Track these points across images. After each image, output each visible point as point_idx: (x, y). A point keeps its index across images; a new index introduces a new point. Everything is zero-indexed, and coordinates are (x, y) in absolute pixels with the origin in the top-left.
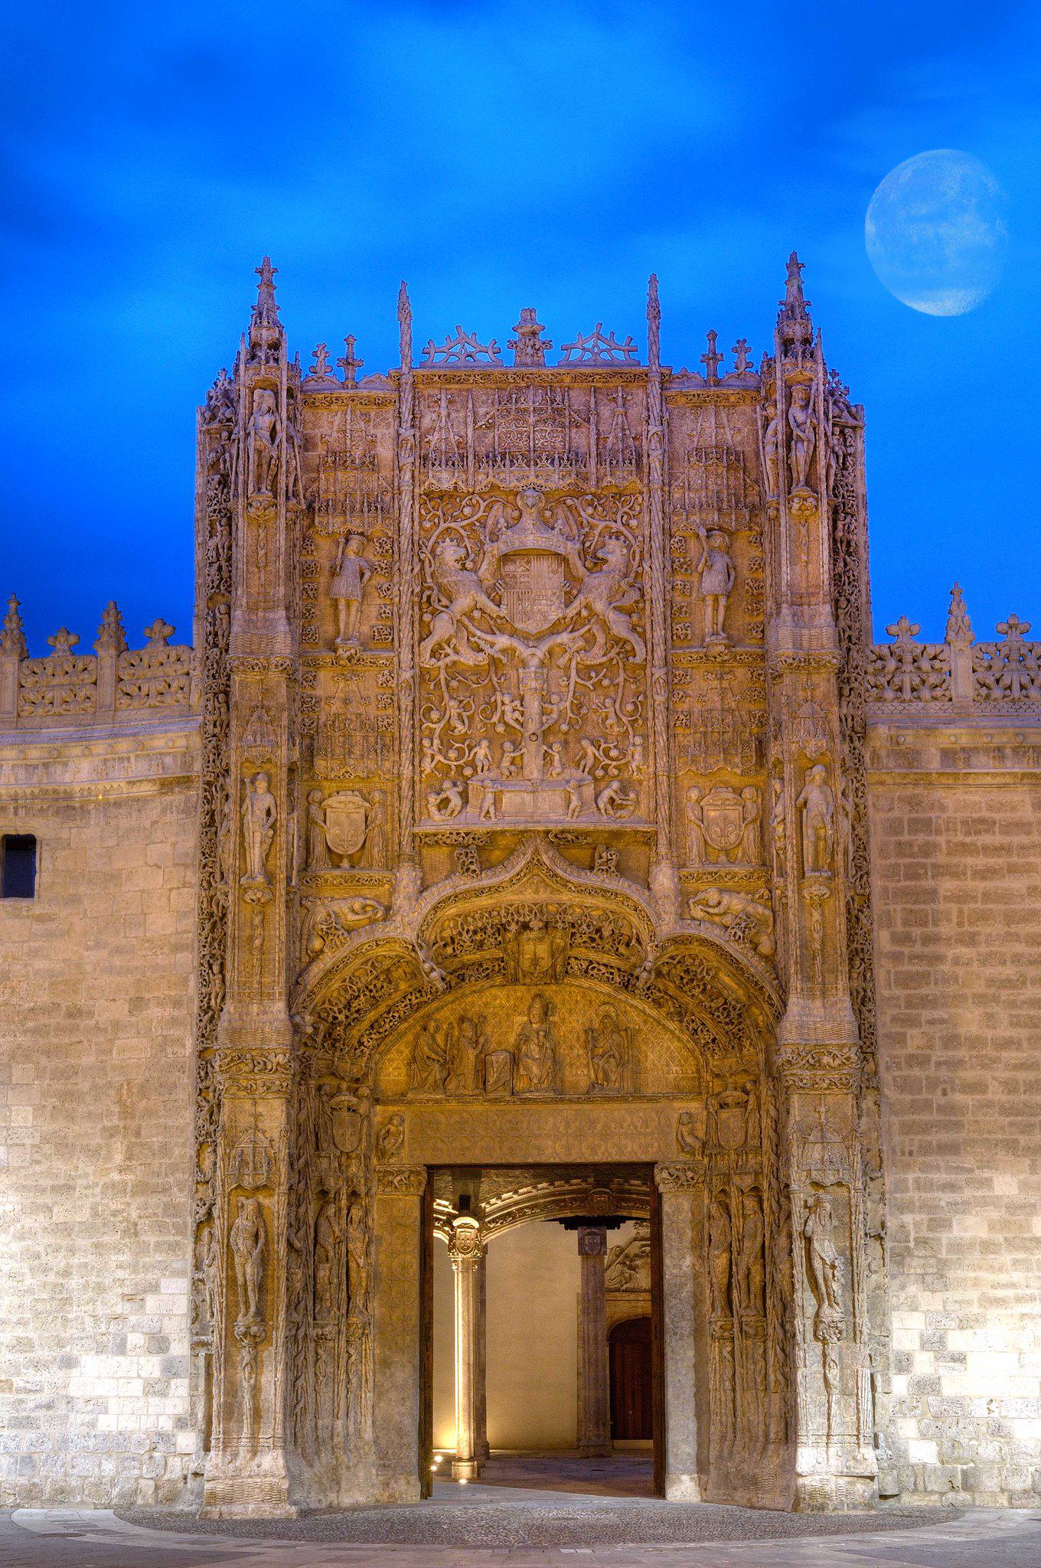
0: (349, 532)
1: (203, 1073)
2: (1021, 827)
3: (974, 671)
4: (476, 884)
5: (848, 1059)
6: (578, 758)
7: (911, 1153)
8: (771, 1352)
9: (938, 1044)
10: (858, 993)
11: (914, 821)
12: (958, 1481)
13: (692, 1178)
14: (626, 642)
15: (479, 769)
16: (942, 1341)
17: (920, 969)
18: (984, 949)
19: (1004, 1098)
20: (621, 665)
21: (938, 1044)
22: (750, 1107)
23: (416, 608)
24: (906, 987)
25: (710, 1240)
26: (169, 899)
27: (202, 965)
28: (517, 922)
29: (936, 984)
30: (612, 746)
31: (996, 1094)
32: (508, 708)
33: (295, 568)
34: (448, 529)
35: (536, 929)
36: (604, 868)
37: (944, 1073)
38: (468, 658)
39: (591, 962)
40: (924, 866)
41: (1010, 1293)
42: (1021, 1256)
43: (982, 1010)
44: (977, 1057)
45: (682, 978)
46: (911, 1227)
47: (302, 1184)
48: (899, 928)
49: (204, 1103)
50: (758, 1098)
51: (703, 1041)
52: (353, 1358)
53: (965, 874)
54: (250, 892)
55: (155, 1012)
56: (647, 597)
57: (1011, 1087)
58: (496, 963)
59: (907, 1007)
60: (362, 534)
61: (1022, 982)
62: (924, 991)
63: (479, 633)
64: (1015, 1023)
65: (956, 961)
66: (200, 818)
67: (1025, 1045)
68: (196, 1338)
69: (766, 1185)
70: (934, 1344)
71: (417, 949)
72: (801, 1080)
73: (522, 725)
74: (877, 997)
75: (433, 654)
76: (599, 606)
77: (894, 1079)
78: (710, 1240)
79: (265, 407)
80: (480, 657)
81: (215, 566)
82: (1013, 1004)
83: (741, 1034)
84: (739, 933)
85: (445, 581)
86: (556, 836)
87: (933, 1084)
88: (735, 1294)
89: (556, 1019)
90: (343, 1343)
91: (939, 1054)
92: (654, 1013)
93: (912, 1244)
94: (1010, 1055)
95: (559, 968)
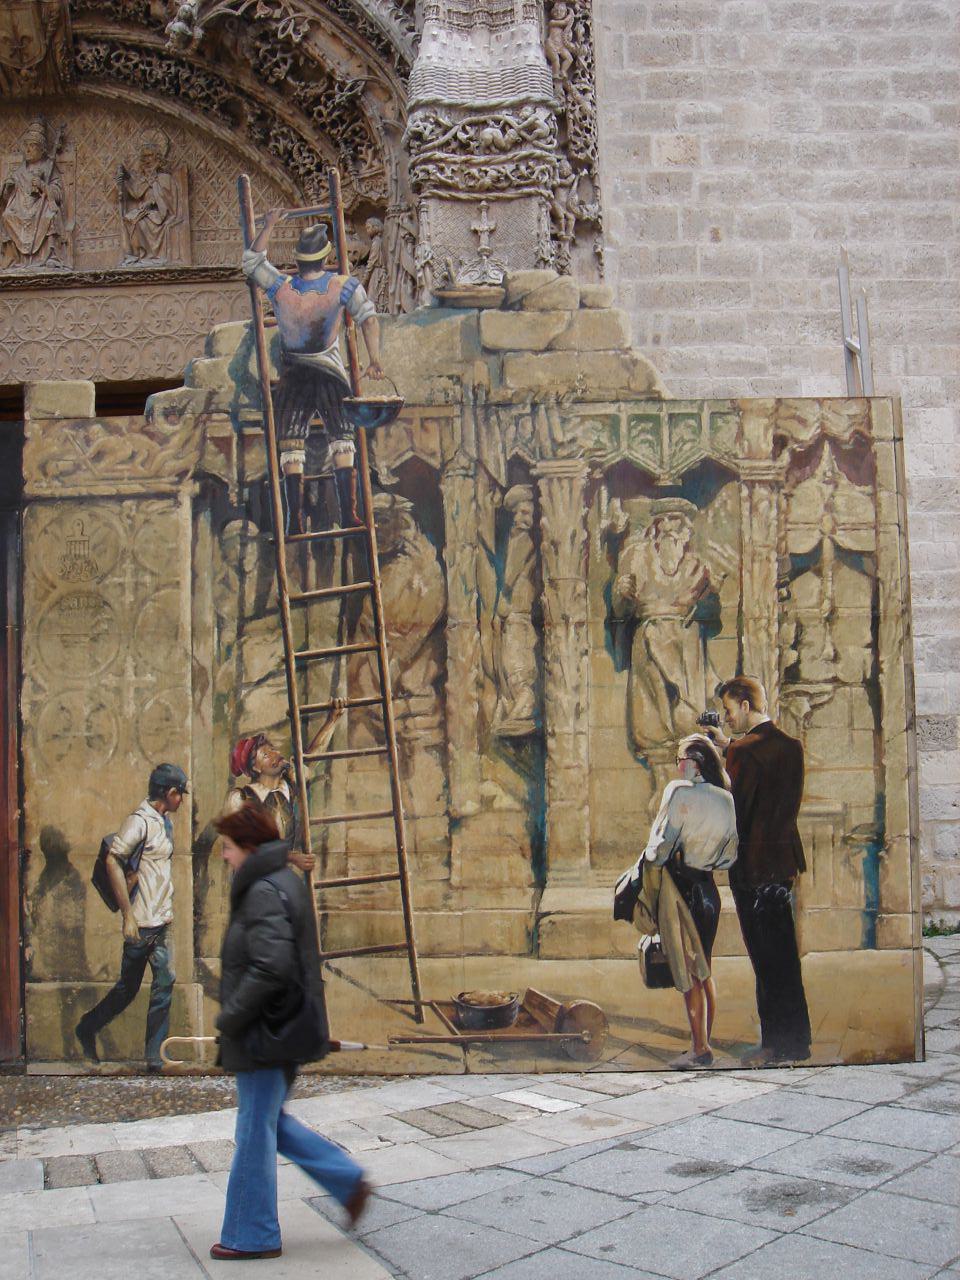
5: (531, 128)
7: (657, 340)
9: (705, 157)
10: (562, 59)
17: (674, 33)
19: (817, 245)
21: (705, 157)
22: (371, 263)
24: (648, 61)
29: (701, 57)
37: (715, 205)
39: (113, 45)
43: (778, 99)
44: (771, 177)
50: (383, 249)
51: (302, 171)
57: (829, 229)
59: (649, 96)
61: (847, 53)
62: (679, 69)
64: (836, 121)
67: (853, 156)
72: (442, 170)
74: (597, 74)
77: (628, 215)
82: (831, 92)
83: (357, 140)
89: (68, 156)
91: (706, 171)
92: (226, 134)
94: (830, 174)
95: (59, 60)
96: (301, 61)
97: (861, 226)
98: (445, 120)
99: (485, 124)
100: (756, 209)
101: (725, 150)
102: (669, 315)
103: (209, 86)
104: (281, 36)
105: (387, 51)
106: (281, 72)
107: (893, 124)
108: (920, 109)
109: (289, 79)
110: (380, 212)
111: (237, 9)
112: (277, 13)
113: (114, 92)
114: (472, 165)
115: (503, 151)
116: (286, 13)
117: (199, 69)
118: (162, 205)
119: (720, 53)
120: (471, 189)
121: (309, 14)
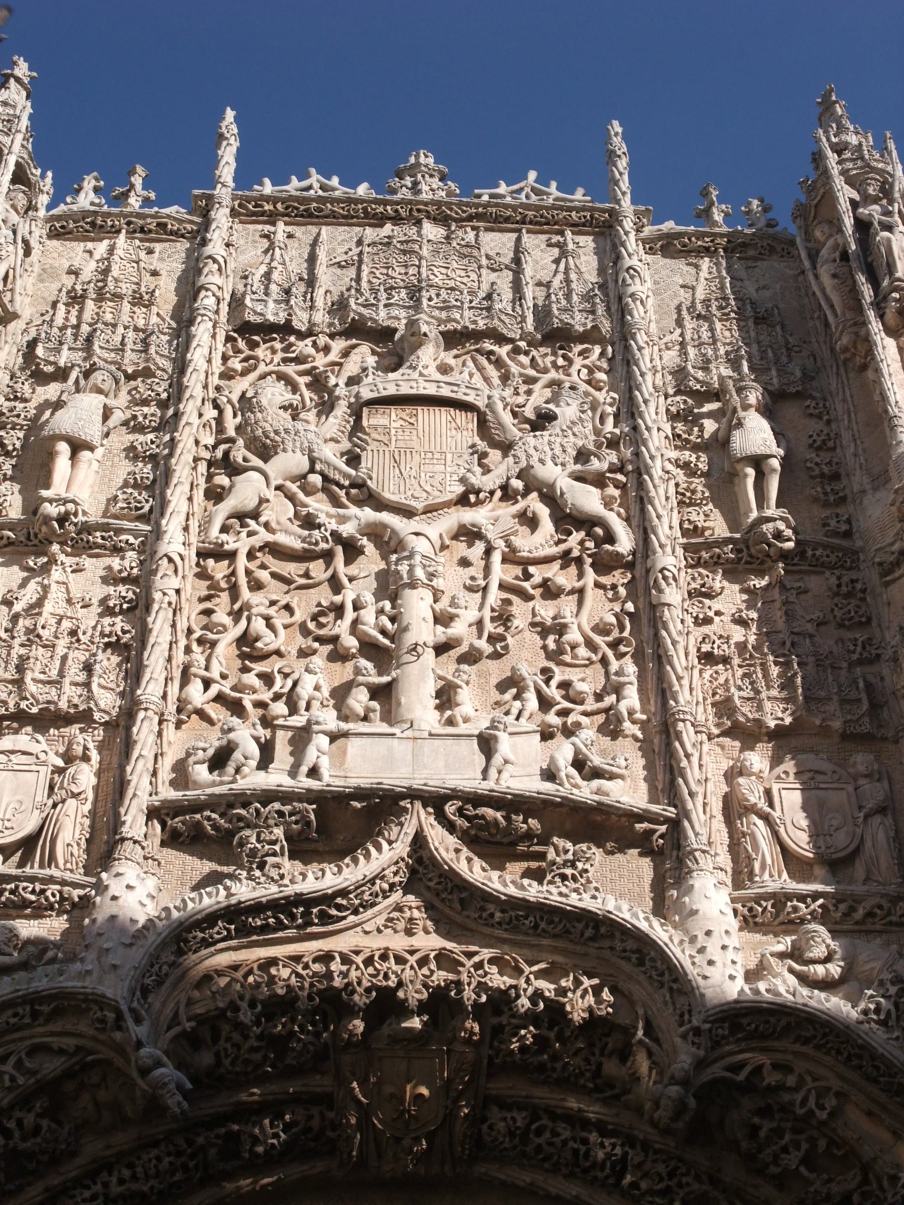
15: (302, 704)
30: (574, 679)
32: (369, 615)
36: (569, 871)
39: (535, 1113)
45: (754, 1131)
58: (315, 1111)
63: (316, 505)
71: (130, 1022)
73: (392, 639)
75: (225, 529)
76: (549, 472)
80: (316, 532)
86: (460, 812)
96: (822, 1143)
103: (671, 1175)
104: (801, 1112)
106: (792, 1159)
109: (803, 1169)
111: (738, 1075)
112: (791, 1081)
113: (525, 1177)
116: (801, 1081)
117: (656, 1152)
121: (836, 1084)
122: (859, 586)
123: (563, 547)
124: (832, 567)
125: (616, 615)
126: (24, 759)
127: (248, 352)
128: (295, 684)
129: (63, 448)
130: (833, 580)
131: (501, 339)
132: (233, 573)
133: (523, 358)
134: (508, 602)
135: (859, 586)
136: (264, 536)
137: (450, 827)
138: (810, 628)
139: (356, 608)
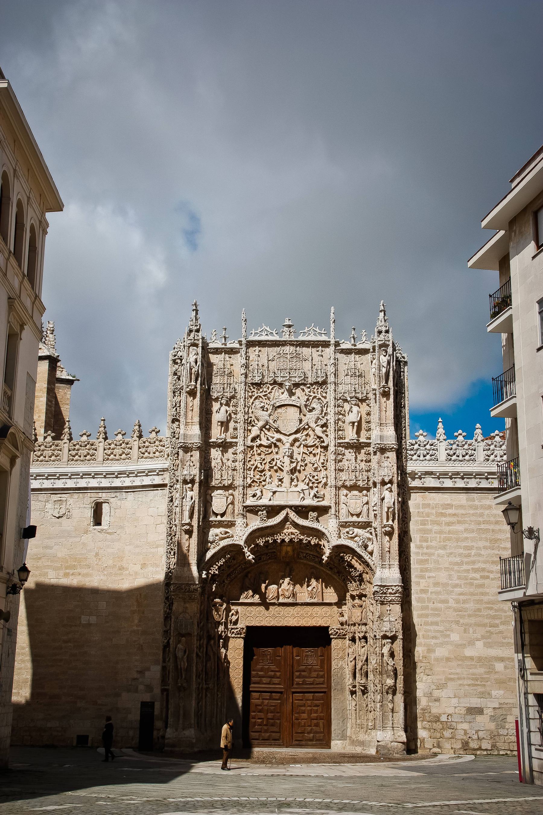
0: (223, 397)
1: (167, 591)
2: (461, 507)
3: (446, 450)
4: (265, 525)
5: (398, 591)
6: (303, 479)
8: (369, 697)
11: (423, 504)
12: (435, 745)
13: (343, 633)
14: (321, 438)
16: (431, 694)
18: (448, 551)
20: (319, 446)
23: (246, 426)
25: (348, 655)
26: (156, 528)
27: (167, 552)
28: (280, 539)
31: (452, 603)
32: (278, 462)
33: (203, 410)
34: (257, 397)
35: (287, 542)
36: (312, 520)
37: (434, 596)
38: (264, 442)
39: (307, 554)
40: (427, 520)
41: (456, 676)
42: (460, 663)
45: (340, 560)
46: (421, 652)
47: (202, 633)
48: (418, 543)
49: (167, 602)
52: (219, 696)
53: (442, 524)
54: (185, 527)
55: (150, 569)
56: (329, 422)
57: (457, 601)
60: (227, 398)
61: (462, 563)
64: (459, 578)
65: (438, 555)
66: (167, 500)
68: (163, 687)
69: (368, 637)
70: (429, 695)
73: (283, 467)
75: (252, 441)
76: (313, 425)
78: (348, 655)
79: (194, 353)
81: (175, 408)
82: (459, 572)
84: (360, 544)
85: (256, 415)
87: (429, 600)
88: (357, 675)
90: (216, 691)
92: (329, 572)
93: (421, 658)
97: (464, 602)
98: (382, 589)
99: (389, 589)
100: (442, 597)
101: (436, 584)
102: (424, 619)
105: (368, 565)
107: (471, 579)
108: (477, 576)
110: (365, 596)
114: (386, 596)
115: (393, 594)
118: (316, 587)
119: (435, 562)
120: (386, 602)
122: (370, 452)
123: (315, 442)
124: (366, 446)
125: (324, 460)
126: (221, 496)
127: (253, 390)
128: (266, 478)
129: (219, 424)
130: (365, 450)
131: (305, 385)
132: (254, 451)
133: (309, 390)
134: (304, 458)
135: (370, 452)
136: (259, 442)
137: (293, 511)
138: (360, 461)
139: (277, 459)
